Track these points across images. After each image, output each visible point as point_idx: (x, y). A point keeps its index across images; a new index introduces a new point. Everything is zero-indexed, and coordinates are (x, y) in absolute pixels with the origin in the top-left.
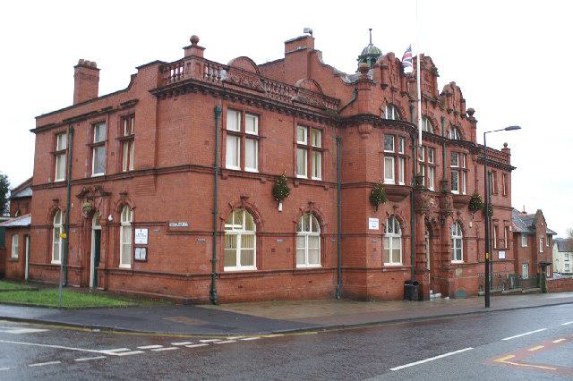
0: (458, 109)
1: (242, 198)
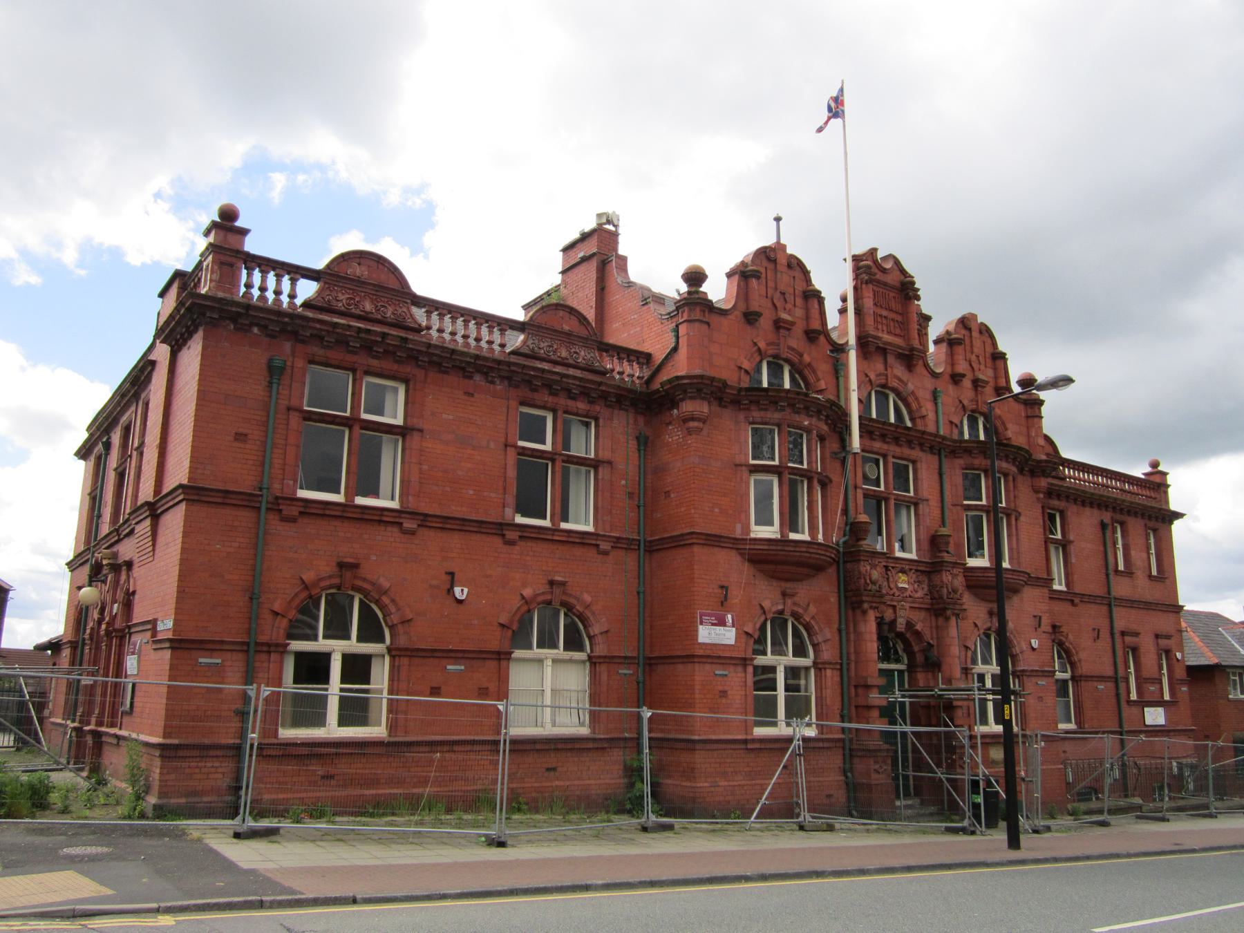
0: (986, 374)
1: (341, 566)
